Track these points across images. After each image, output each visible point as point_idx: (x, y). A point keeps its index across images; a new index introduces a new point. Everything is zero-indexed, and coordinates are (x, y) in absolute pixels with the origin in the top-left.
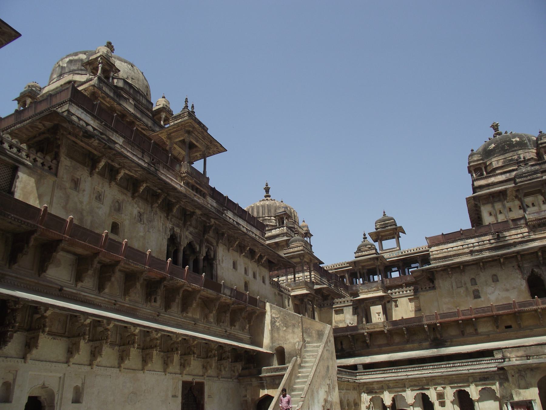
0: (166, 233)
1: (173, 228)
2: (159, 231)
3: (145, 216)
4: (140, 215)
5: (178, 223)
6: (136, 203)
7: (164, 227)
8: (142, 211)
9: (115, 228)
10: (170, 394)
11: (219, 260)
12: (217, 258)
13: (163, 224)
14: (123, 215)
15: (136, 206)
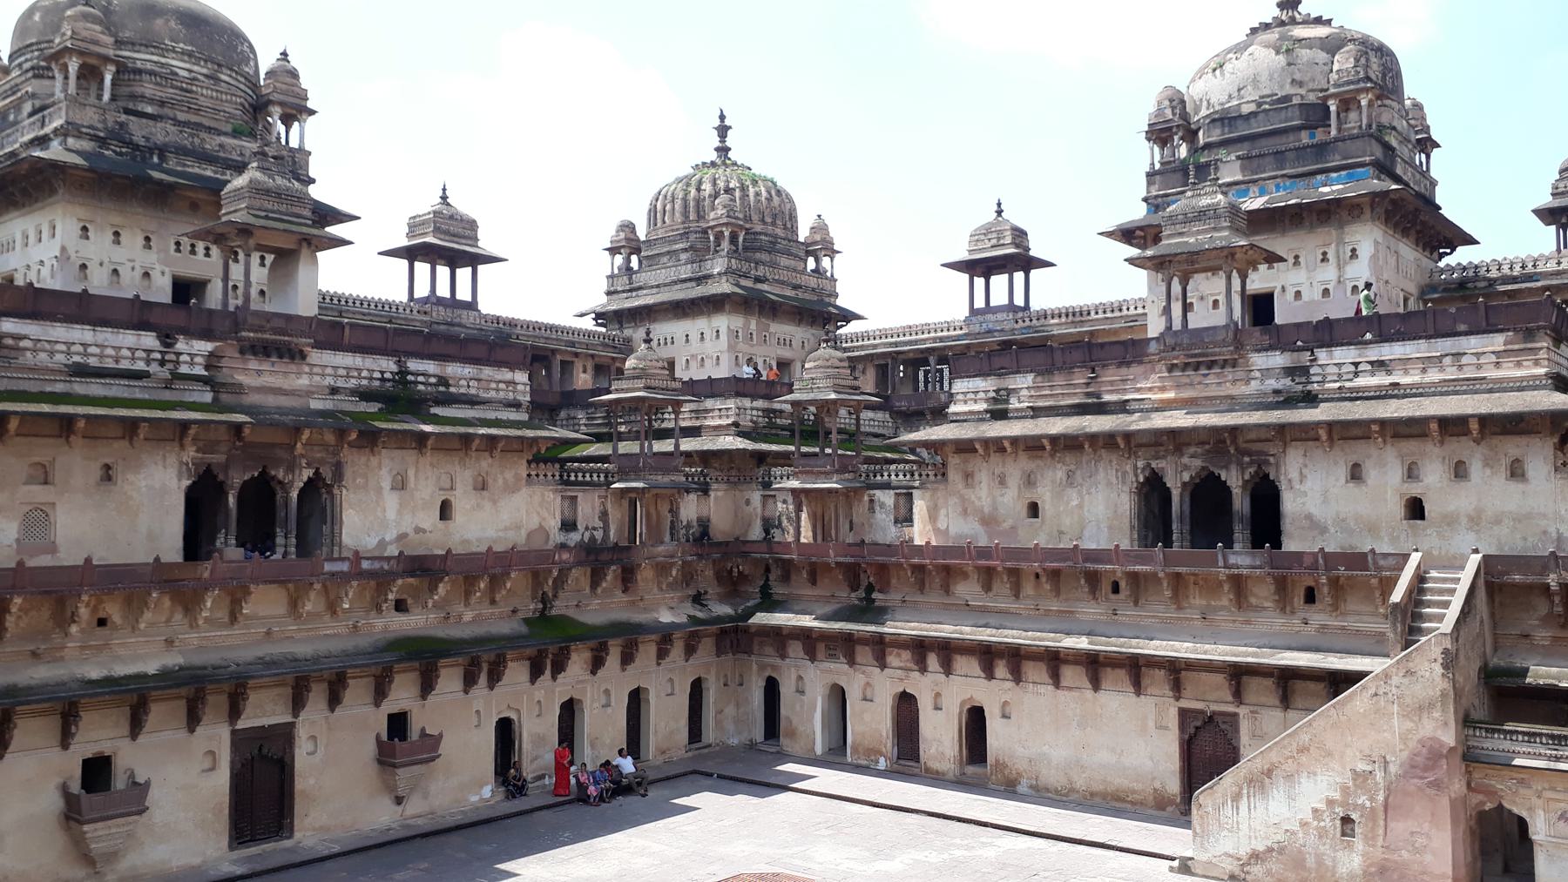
0: (1124, 483)
1: (1149, 465)
2: (1109, 484)
3: (1078, 473)
4: (1070, 475)
5: (1153, 453)
6: (1058, 462)
7: (1120, 474)
8: (1073, 467)
9: (1034, 510)
10: (1151, 724)
11: (1290, 480)
12: (1282, 478)
13: (1117, 471)
14: (1039, 489)
15: (1059, 466)
